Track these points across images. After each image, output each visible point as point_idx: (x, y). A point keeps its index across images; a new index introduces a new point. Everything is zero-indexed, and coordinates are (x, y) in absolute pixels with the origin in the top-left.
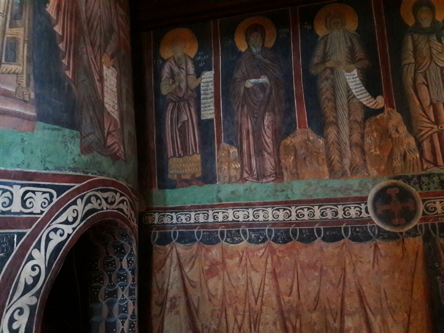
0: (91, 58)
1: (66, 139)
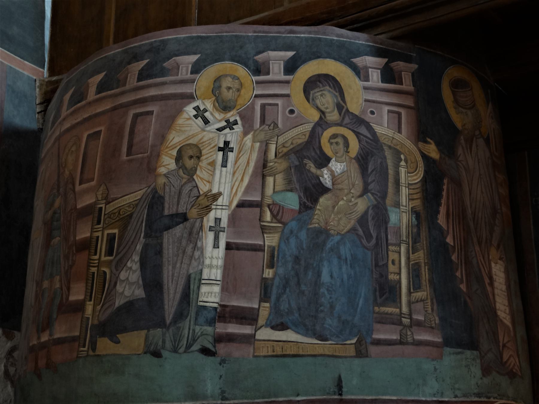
0: (480, 259)
1: (468, 361)
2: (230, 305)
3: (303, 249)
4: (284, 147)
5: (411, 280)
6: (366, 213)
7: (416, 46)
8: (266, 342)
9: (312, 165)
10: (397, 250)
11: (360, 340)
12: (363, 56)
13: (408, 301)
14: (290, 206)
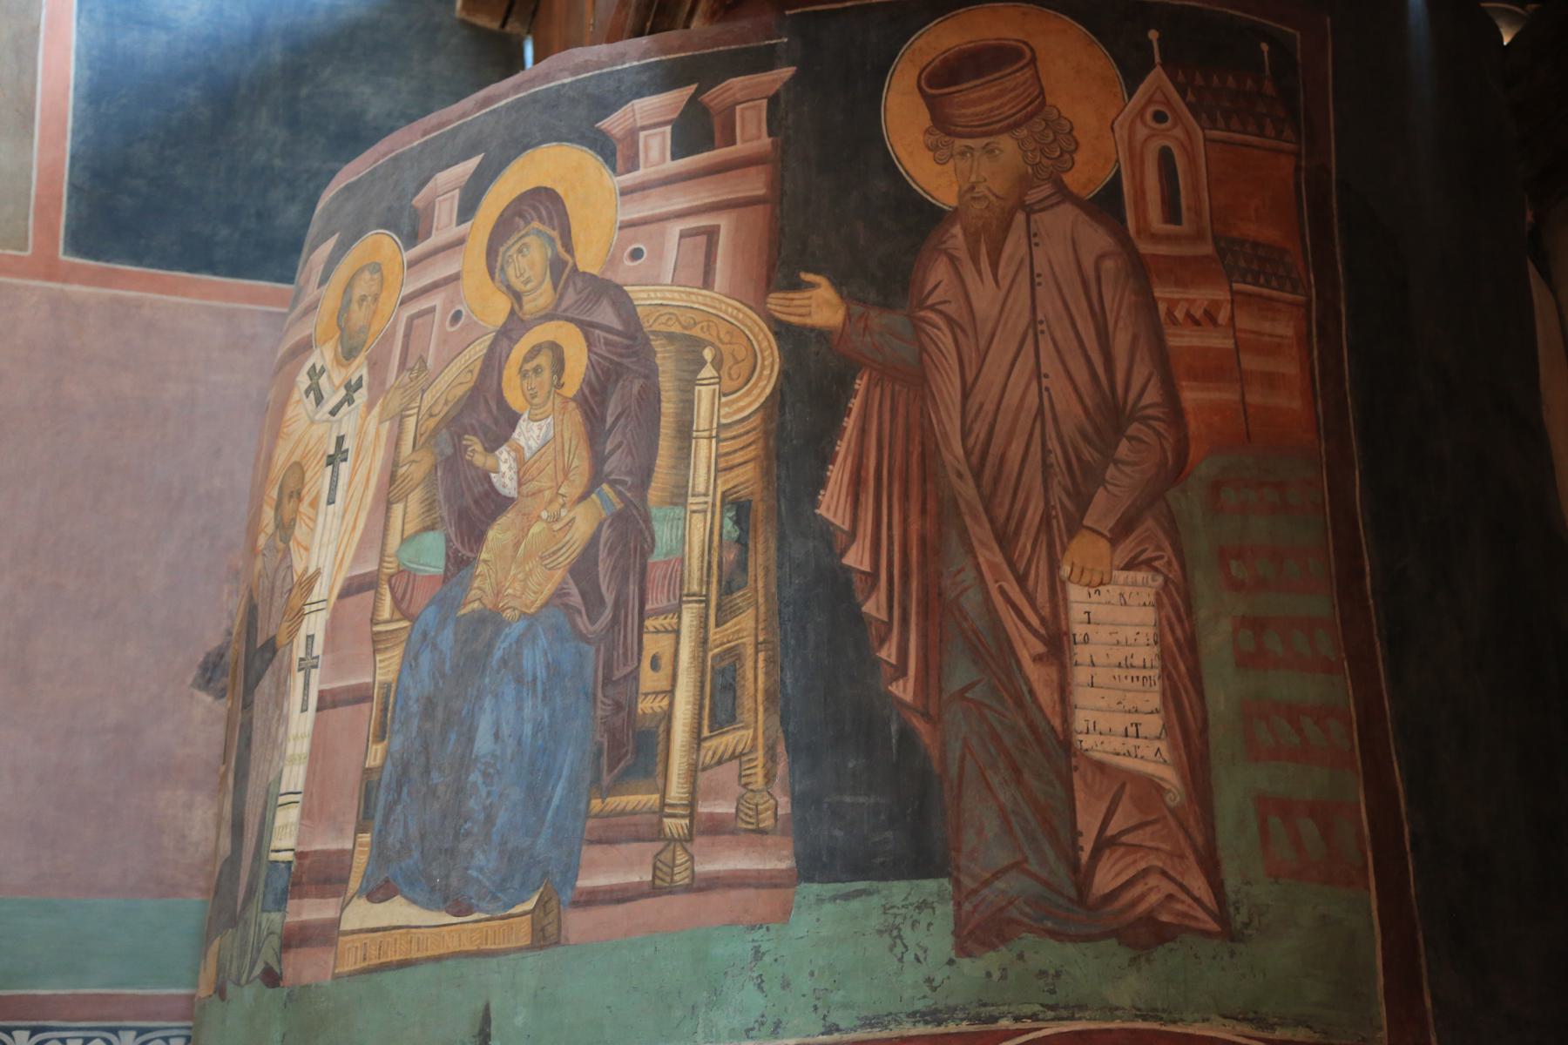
0: (1002, 591)
2: (311, 852)
3: (443, 676)
4: (431, 416)
5: (707, 702)
6: (593, 542)
7: (787, 13)
8: (355, 936)
9: (479, 447)
10: (670, 624)
11: (546, 899)
12: (627, 102)
13: (690, 764)
14: (427, 568)
